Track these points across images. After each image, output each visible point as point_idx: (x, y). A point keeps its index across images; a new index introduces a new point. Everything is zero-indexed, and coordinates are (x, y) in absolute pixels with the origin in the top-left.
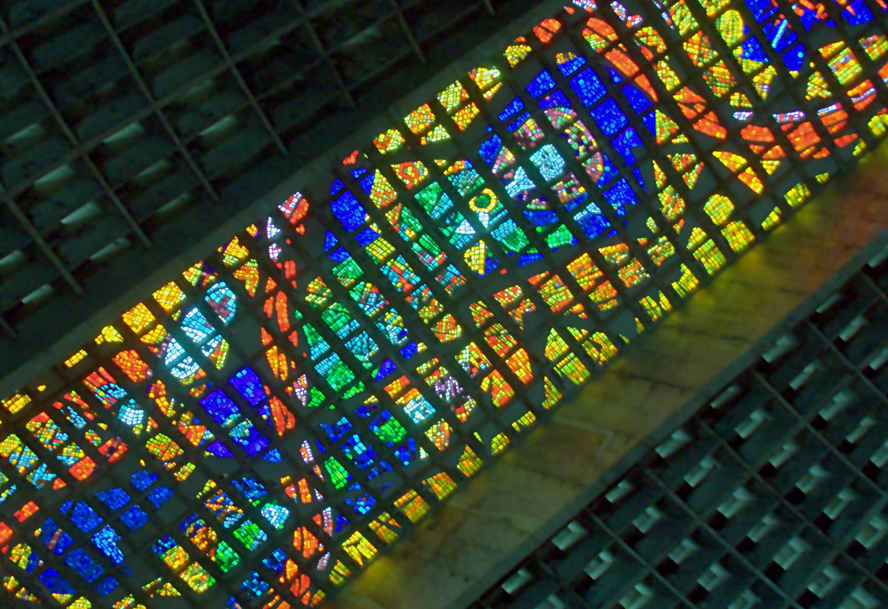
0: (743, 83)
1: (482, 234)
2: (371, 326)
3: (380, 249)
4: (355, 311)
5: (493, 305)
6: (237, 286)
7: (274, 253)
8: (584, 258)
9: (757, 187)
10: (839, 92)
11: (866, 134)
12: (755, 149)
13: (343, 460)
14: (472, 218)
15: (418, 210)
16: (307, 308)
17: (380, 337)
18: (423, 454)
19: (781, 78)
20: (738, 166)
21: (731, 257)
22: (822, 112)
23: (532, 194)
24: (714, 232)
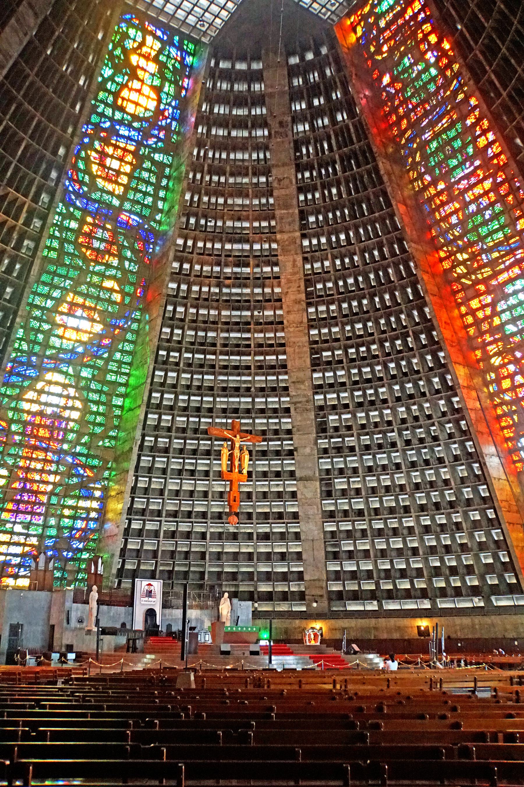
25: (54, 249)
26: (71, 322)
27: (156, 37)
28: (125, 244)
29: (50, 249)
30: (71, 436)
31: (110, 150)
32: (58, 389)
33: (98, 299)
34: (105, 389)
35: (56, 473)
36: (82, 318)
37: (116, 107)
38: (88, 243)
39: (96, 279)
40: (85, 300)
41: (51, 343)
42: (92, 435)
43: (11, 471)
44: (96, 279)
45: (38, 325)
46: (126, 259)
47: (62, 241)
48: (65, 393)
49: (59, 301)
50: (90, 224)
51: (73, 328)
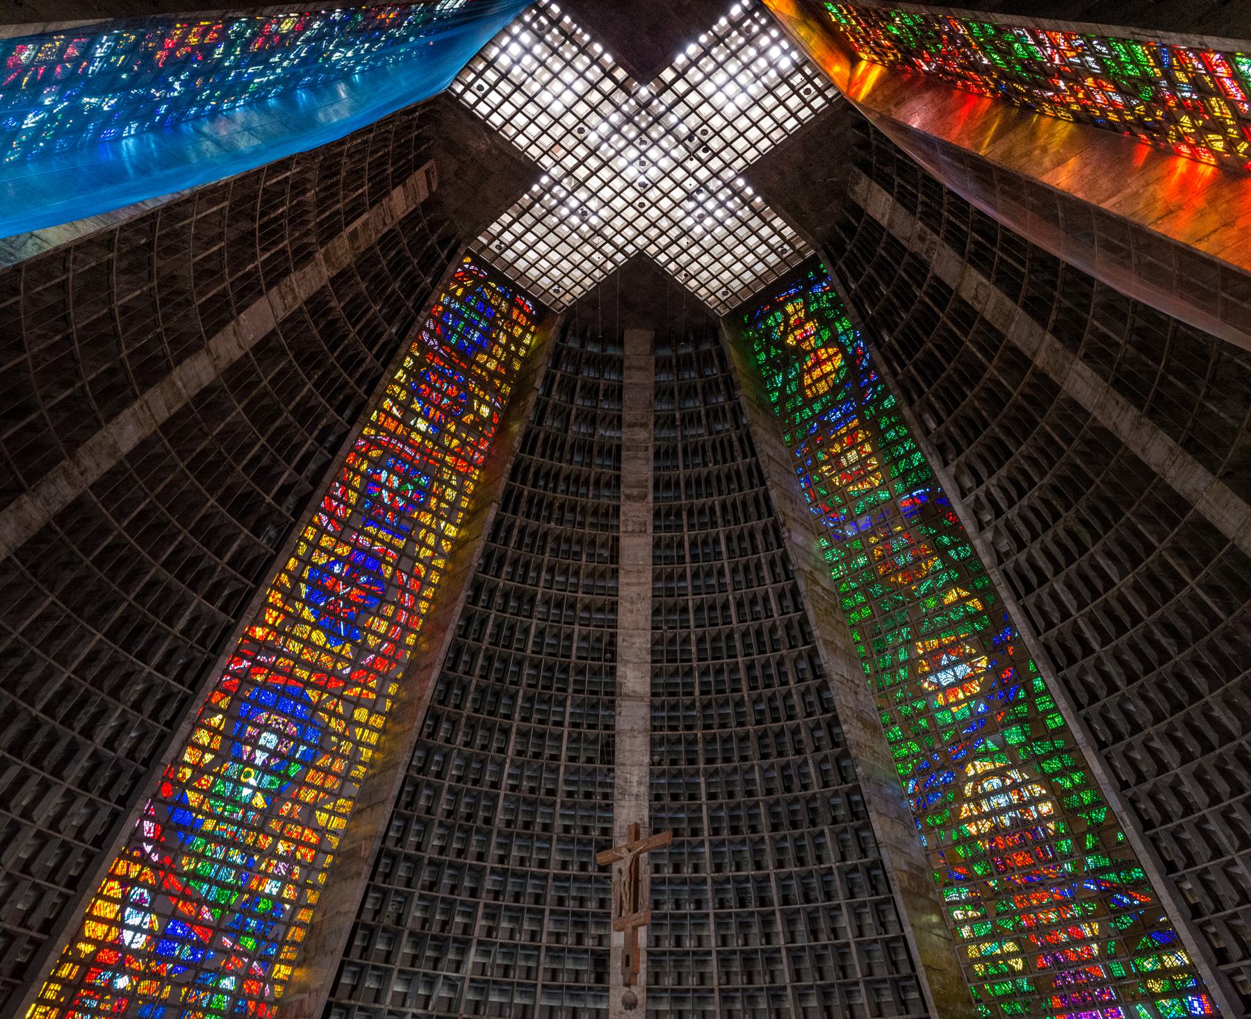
0: (339, 657)
1: (256, 789)
2: (225, 863)
3: (209, 825)
4: (213, 861)
5: (279, 818)
6: (144, 885)
7: (155, 858)
8: (312, 772)
9: (372, 696)
10: (384, 637)
13: (248, 934)
14: (248, 785)
15: (218, 796)
16: (186, 874)
17: (233, 865)
18: (287, 907)
23: (269, 759)
24: (365, 726)
25: (863, 605)
26: (946, 678)
28: (932, 531)
29: (857, 608)
30: (1065, 845)
32: (996, 782)
33: (952, 626)
34: (1059, 743)
35: (1086, 918)
36: (952, 665)
37: (808, 403)
39: (931, 603)
40: (939, 639)
41: (940, 723)
42: (1097, 828)
43: (1017, 941)
44: (931, 603)
46: (947, 548)
47: (863, 588)
48: (1008, 782)
49: (912, 663)
51: (951, 685)
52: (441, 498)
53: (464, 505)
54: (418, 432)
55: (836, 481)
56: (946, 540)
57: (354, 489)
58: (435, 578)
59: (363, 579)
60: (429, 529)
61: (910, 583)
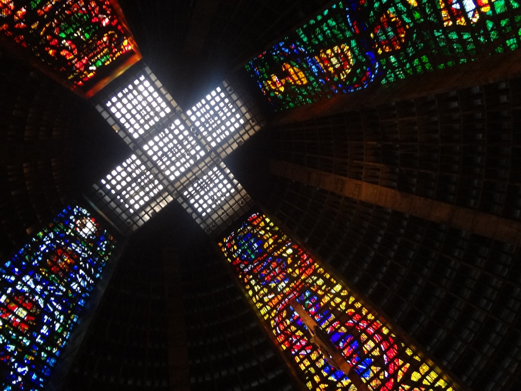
0: (376, 376)
9: (408, 365)
10: (377, 345)
11: (389, 334)
12: (396, 368)
19: (375, 364)
20: (402, 372)
21: (431, 369)
22: (383, 349)
24: (424, 377)
25: (420, 61)
27: (264, 87)
28: (372, 13)
29: (422, 64)
31: (331, 69)
38: (395, 41)
39: (417, 15)
40: (441, 10)
45: (493, 33)
47: (411, 60)
50: (382, 50)
52: (320, 287)
53: (328, 276)
54: (284, 288)
55: (348, 71)
56: (376, 5)
57: (296, 331)
58: (358, 305)
59: (341, 344)
60: (332, 299)
61: (405, 29)
